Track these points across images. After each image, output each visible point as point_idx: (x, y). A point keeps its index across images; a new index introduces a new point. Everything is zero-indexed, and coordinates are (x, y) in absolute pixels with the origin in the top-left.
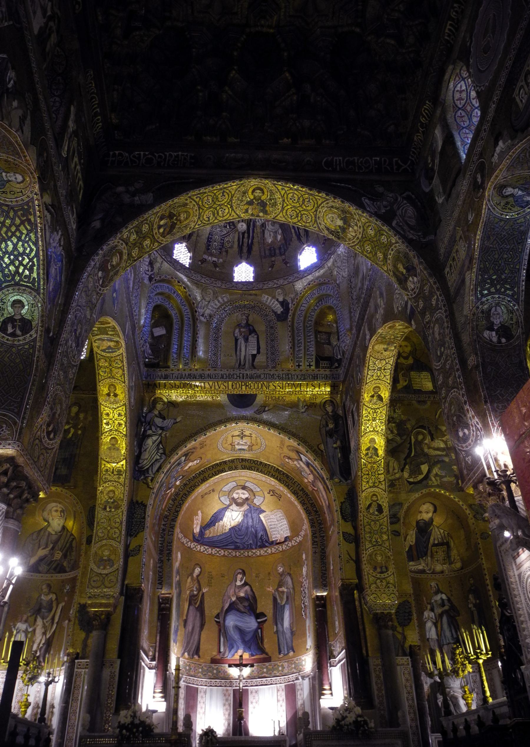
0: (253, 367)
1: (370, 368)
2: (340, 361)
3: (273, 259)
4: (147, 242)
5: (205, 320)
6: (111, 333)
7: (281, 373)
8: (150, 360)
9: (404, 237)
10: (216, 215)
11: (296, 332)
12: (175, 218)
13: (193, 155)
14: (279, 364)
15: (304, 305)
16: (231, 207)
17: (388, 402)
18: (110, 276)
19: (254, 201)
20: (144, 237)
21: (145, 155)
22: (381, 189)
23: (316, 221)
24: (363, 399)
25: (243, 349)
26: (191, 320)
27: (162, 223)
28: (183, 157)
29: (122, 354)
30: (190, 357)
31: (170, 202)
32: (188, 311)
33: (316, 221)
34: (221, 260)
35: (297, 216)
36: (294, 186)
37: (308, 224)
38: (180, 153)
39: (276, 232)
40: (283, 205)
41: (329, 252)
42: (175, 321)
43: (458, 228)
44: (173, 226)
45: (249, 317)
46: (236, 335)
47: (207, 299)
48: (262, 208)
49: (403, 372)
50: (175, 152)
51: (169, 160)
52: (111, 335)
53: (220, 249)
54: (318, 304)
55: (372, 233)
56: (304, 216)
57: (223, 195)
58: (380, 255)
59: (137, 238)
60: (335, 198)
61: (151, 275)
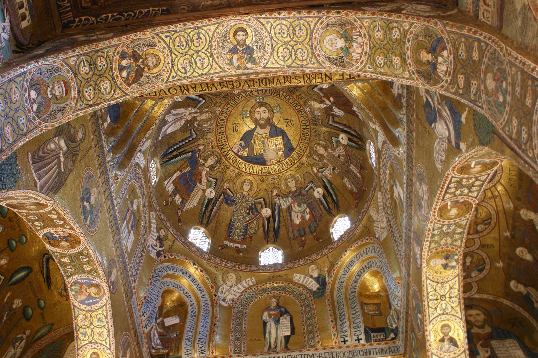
0: (287, 348)
1: (430, 297)
2: (395, 331)
3: (303, 238)
4: (106, 85)
5: (227, 305)
6: (87, 268)
7: (323, 352)
8: (158, 350)
9: (419, 17)
10: (194, 65)
11: (337, 305)
12: (141, 60)
13: (165, 8)
14: (319, 342)
15: (342, 276)
16: (212, 55)
17: (467, 347)
18: (51, 109)
19: (238, 47)
20: (101, 76)
21: (112, 16)
23: (313, 53)
24: (430, 345)
25: (273, 331)
26: (210, 306)
27: (124, 63)
28: (154, 12)
29: (105, 305)
30: (207, 343)
31: (132, 36)
32: (207, 296)
33: (313, 53)
34: (245, 246)
35: (291, 55)
36: (279, 14)
37: (305, 63)
38: (151, 9)
39: (303, 212)
40: (272, 45)
41: (363, 211)
42: (190, 308)
44: (139, 73)
45: (281, 300)
46: (264, 318)
47: (229, 284)
48: (249, 56)
49: (481, 342)
50: (146, 9)
52: (89, 272)
53: (244, 235)
54: (360, 273)
55: (379, 35)
56: (298, 52)
57: (199, 37)
58: (397, 60)
59: (91, 73)
60: (328, 12)
61: (160, 251)
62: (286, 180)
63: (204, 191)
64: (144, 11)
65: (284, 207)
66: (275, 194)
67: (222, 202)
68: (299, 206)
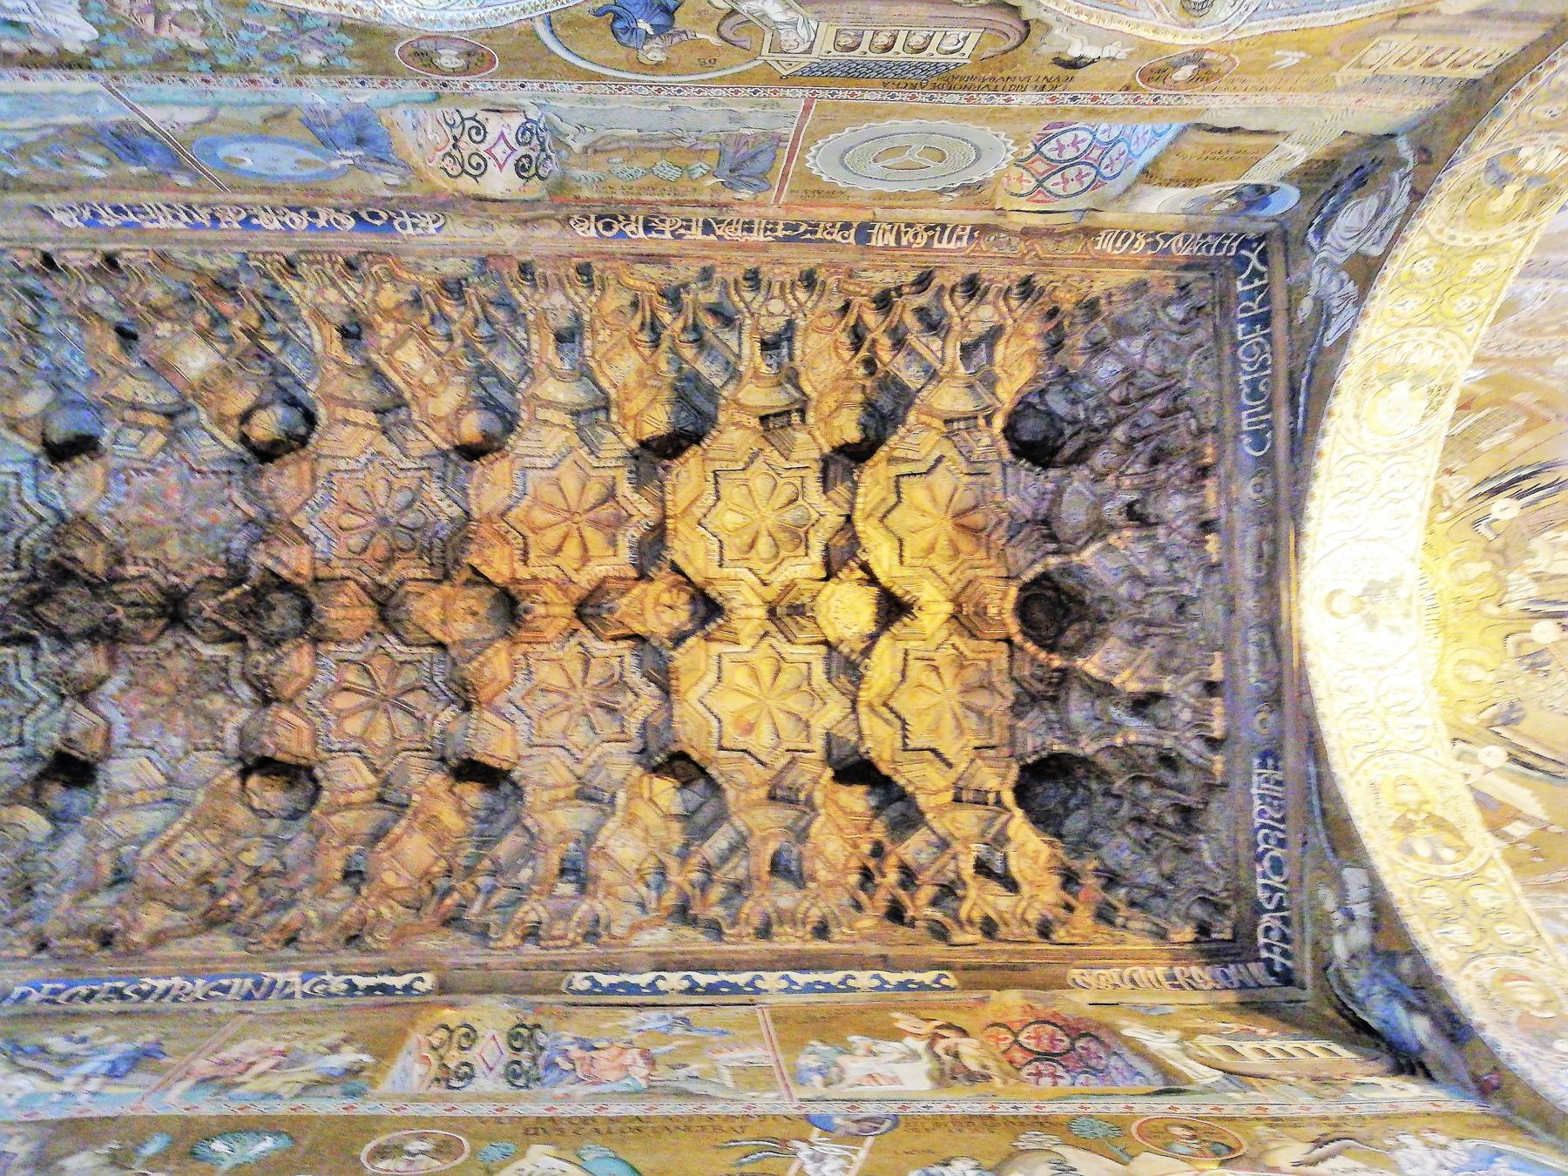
4: (1482, 897)
9: (1408, 214)
12: (1411, 816)
19: (1364, 612)
21: (1265, 876)
22: (1307, 305)
27: (1423, 849)
38: (1254, 791)
43: (1339, 83)
44: (1440, 824)
48: (1385, 592)
51: (1272, 819)
55: (1413, 304)
58: (1479, 266)
62: (1462, 583)
63: (1488, 770)
64: (1257, 805)
65: (1534, 590)
66: (1496, 611)
67: (1516, 732)
68: (1531, 554)
